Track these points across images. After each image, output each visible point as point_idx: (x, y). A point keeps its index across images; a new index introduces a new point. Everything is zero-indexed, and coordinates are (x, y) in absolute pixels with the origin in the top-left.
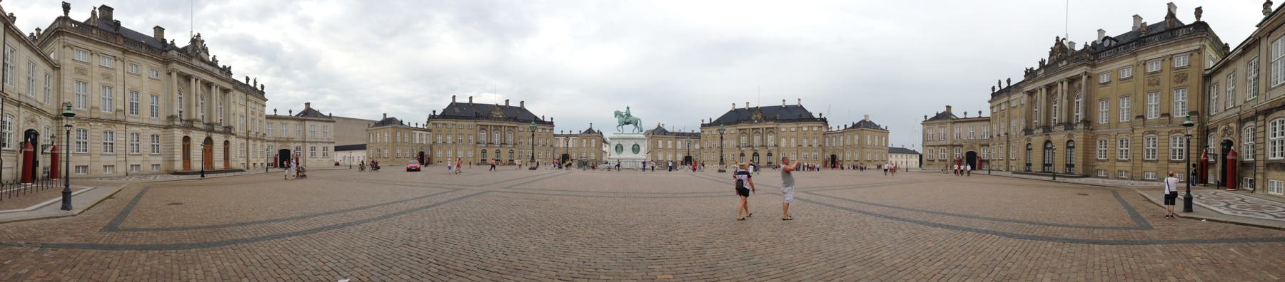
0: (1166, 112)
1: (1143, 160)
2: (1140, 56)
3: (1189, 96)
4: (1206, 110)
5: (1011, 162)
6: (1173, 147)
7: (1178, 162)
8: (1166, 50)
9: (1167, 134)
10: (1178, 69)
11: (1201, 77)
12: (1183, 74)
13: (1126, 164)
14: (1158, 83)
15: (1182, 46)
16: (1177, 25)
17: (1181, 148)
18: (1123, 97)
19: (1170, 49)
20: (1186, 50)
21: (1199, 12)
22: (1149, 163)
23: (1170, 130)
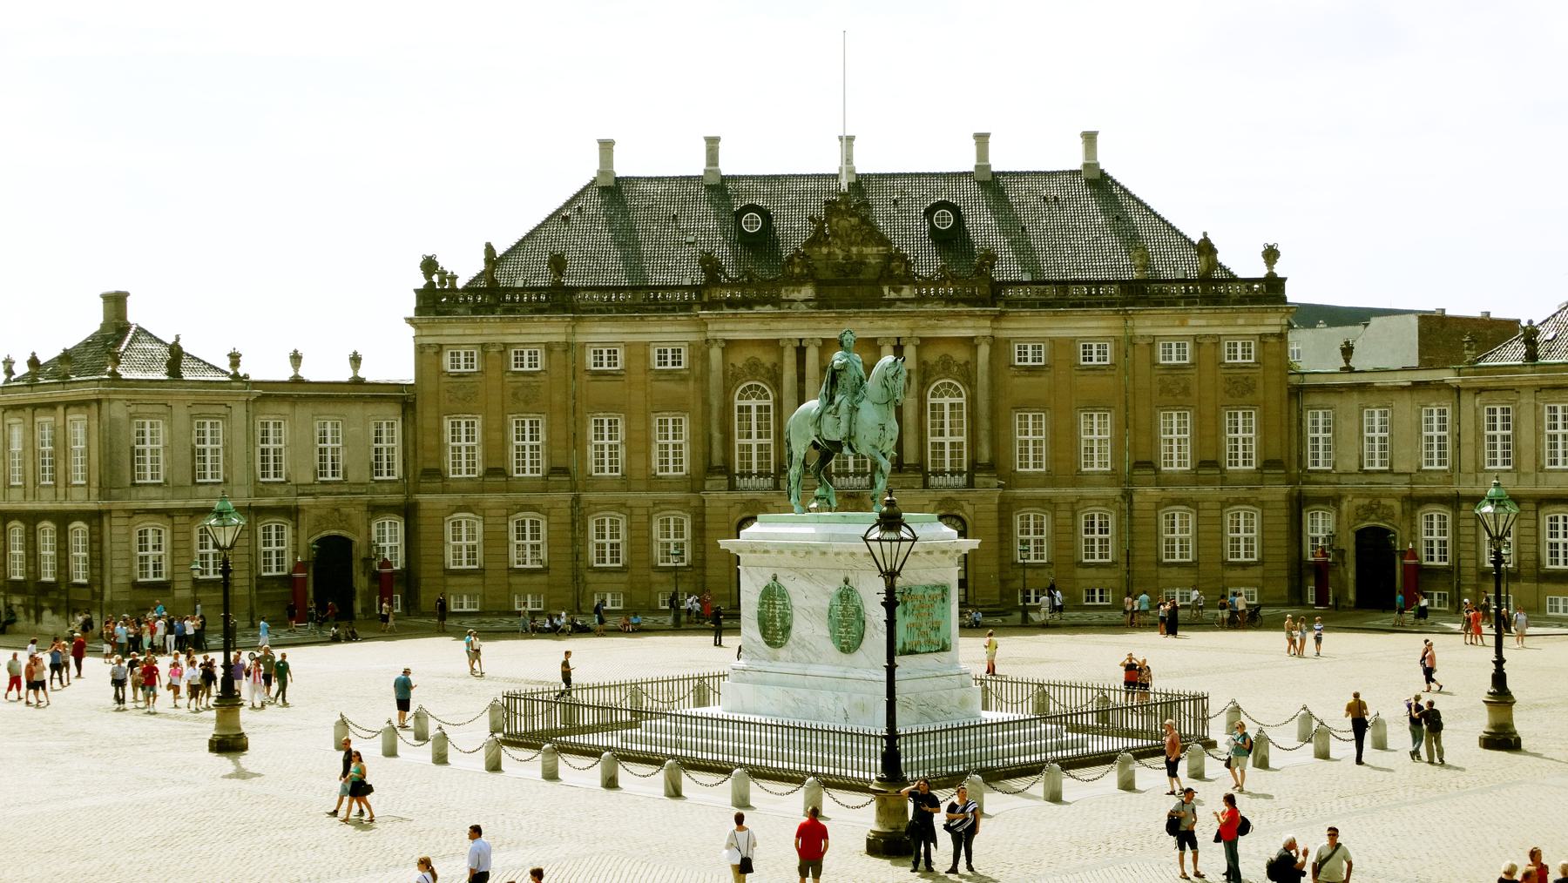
0: (1210, 457)
1: (1159, 563)
2: (1137, 323)
3: (1264, 428)
4: (1294, 456)
5: (590, 577)
6: (1549, 540)
7: (1244, 565)
8: (1203, 322)
9: (1218, 506)
10: (1233, 366)
11: (1285, 393)
12: (1247, 378)
13: (1103, 573)
14: (1186, 391)
15: (1241, 321)
16: (1217, 274)
17: (1443, 538)
18: (1091, 406)
19: (1216, 322)
20: (1252, 330)
21: (1271, 254)
22: (1174, 570)
23: (1224, 498)
